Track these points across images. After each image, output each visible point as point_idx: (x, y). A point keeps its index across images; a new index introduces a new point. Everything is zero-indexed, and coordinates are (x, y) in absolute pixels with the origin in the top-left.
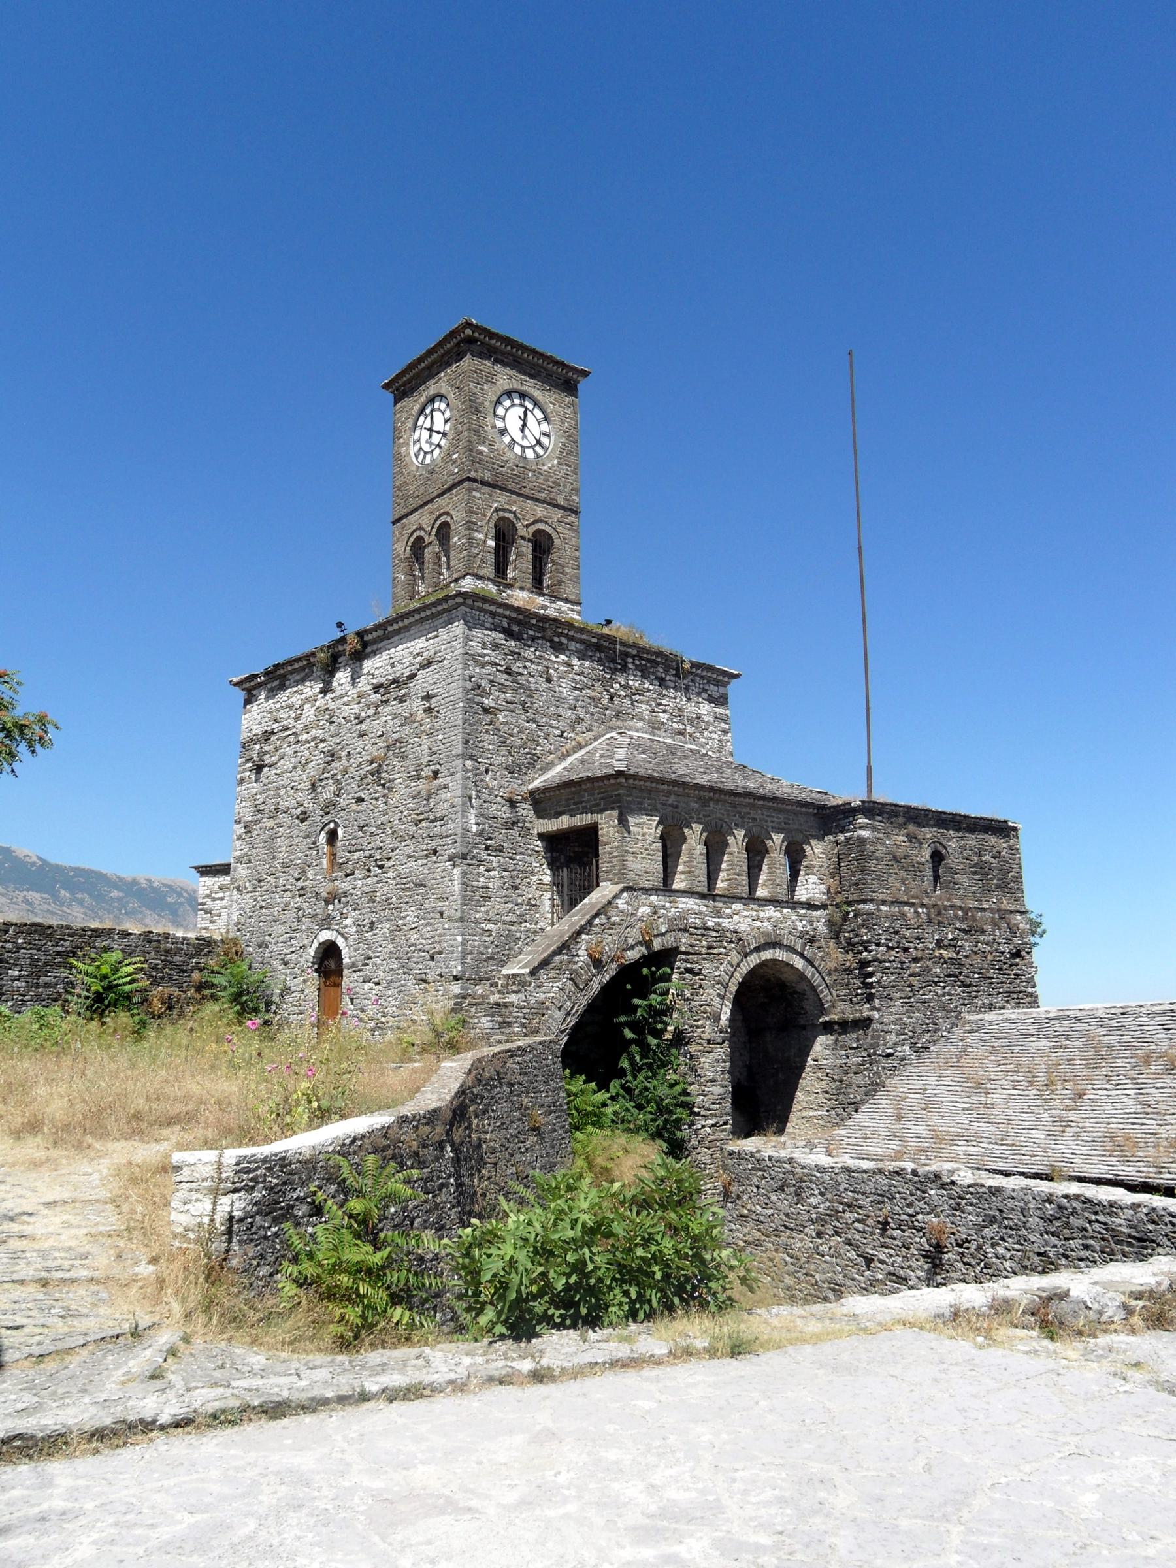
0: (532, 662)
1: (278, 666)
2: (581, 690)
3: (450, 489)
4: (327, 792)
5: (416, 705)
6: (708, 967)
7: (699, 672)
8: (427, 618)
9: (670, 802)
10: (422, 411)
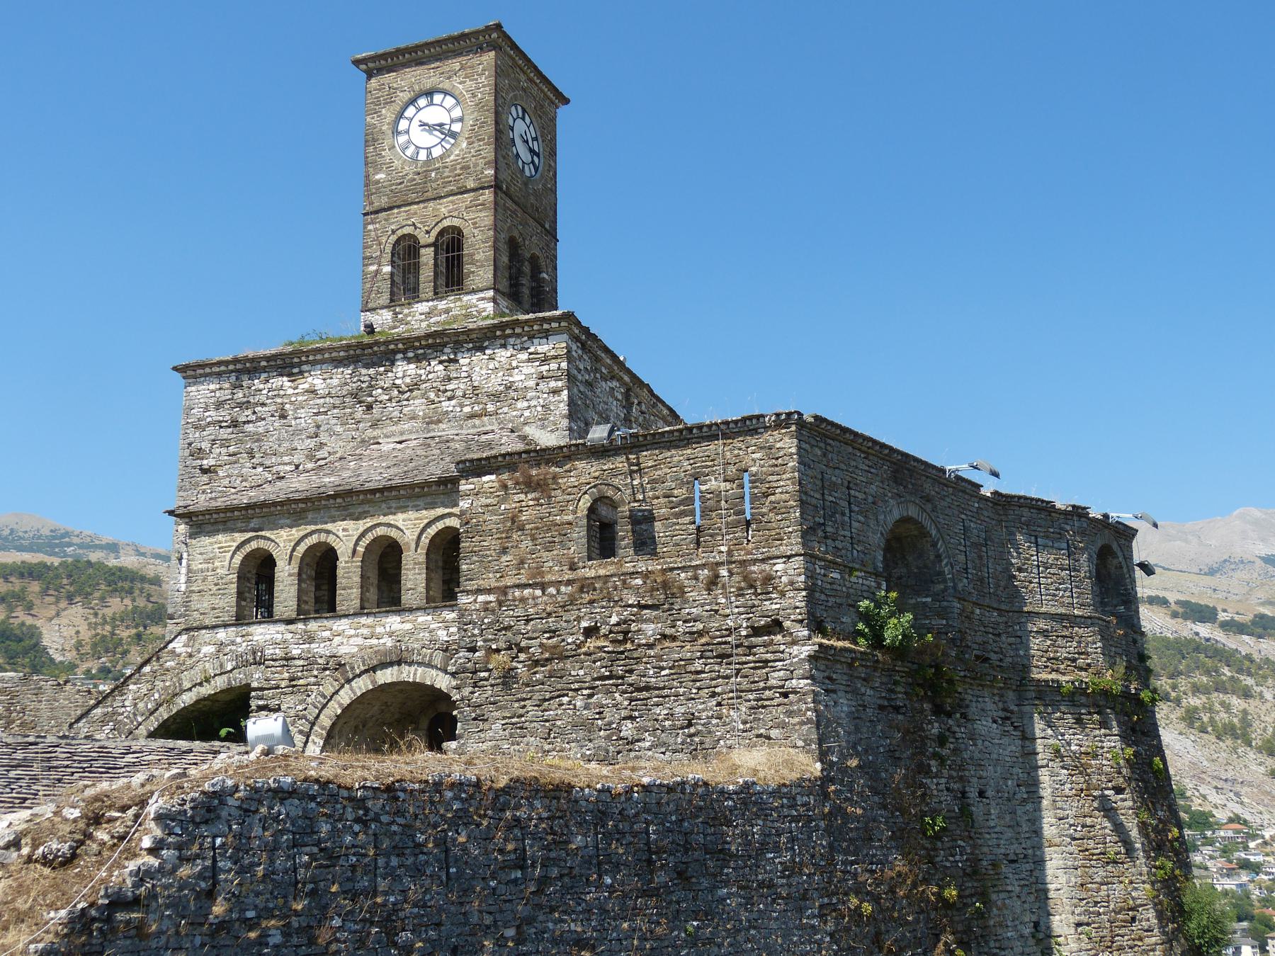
0: (263, 405)
2: (325, 413)
7: (508, 331)
9: (252, 525)
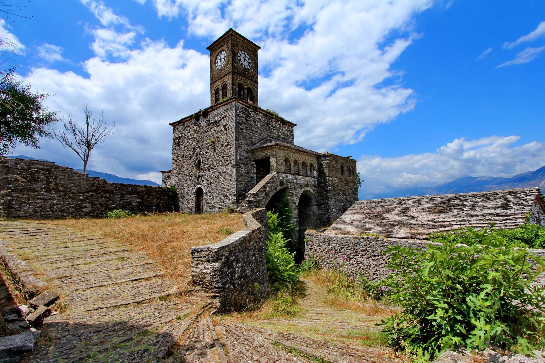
1: (182, 119)
3: (226, 75)
4: (198, 151)
5: (222, 128)
6: (294, 192)
8: (224, 105)
10: (218, 55)
